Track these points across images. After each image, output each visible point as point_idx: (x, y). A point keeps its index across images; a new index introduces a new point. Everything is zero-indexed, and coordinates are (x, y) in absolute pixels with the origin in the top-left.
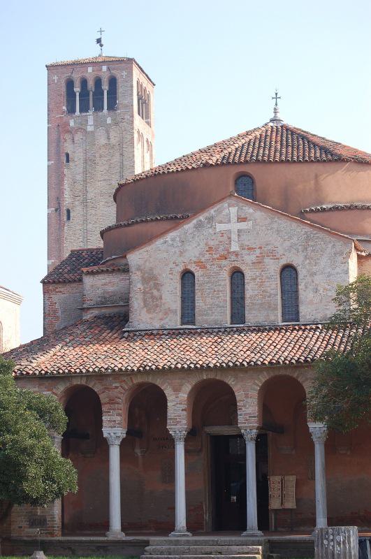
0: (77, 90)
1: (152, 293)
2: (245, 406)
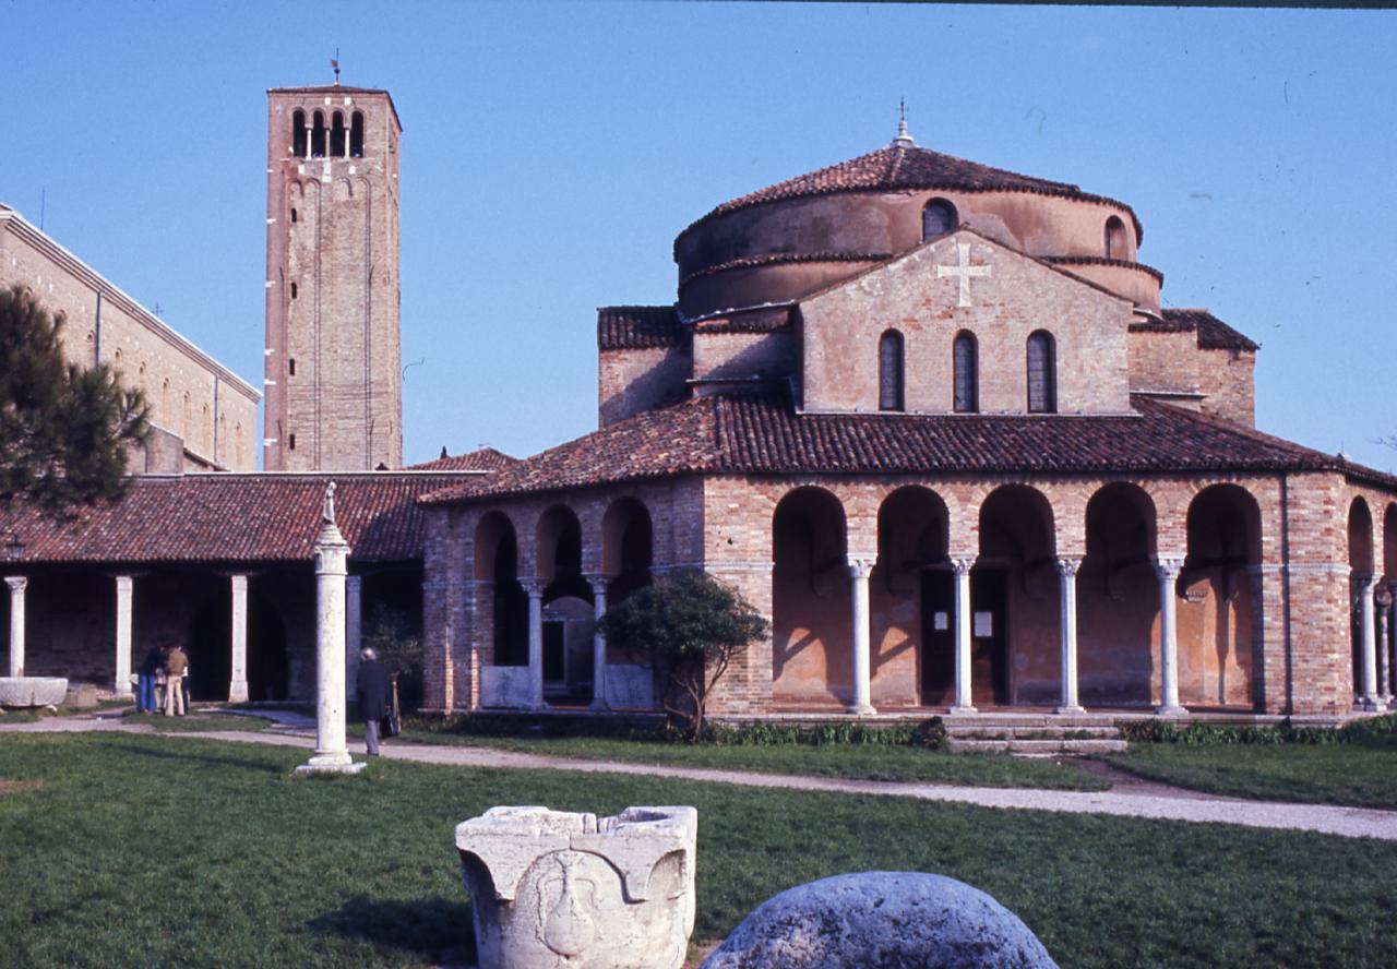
0: (309, 125)
2: (1066, 525)
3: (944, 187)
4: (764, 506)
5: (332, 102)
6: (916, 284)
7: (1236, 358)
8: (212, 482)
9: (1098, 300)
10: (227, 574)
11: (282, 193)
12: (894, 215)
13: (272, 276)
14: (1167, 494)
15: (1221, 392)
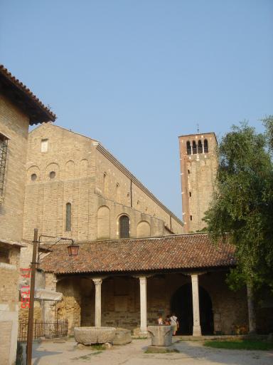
0: (191, 145)
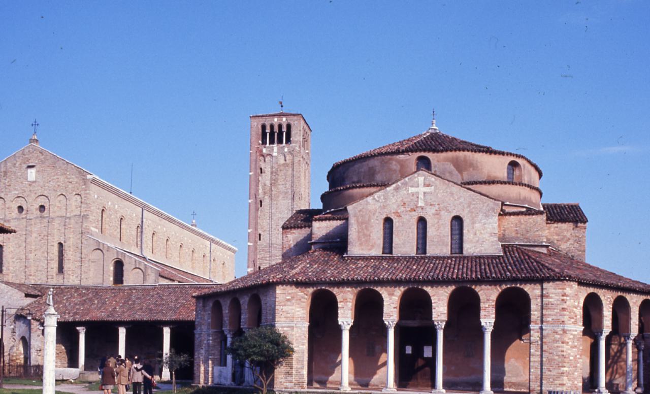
0: (268, 130)
1: (364, 232)
2: (438, 306)
3: (425, 151)
4: (302, 298)
5: (278, 120)
6: (399, 196)
7: (577, 227)
8: (169, 288)
9: (484, 201)
10: (162, 326)
11: (256, 161)
12: (402, 164)
13: (252, 197)
14: (485, 292)
15: (569, 243)
